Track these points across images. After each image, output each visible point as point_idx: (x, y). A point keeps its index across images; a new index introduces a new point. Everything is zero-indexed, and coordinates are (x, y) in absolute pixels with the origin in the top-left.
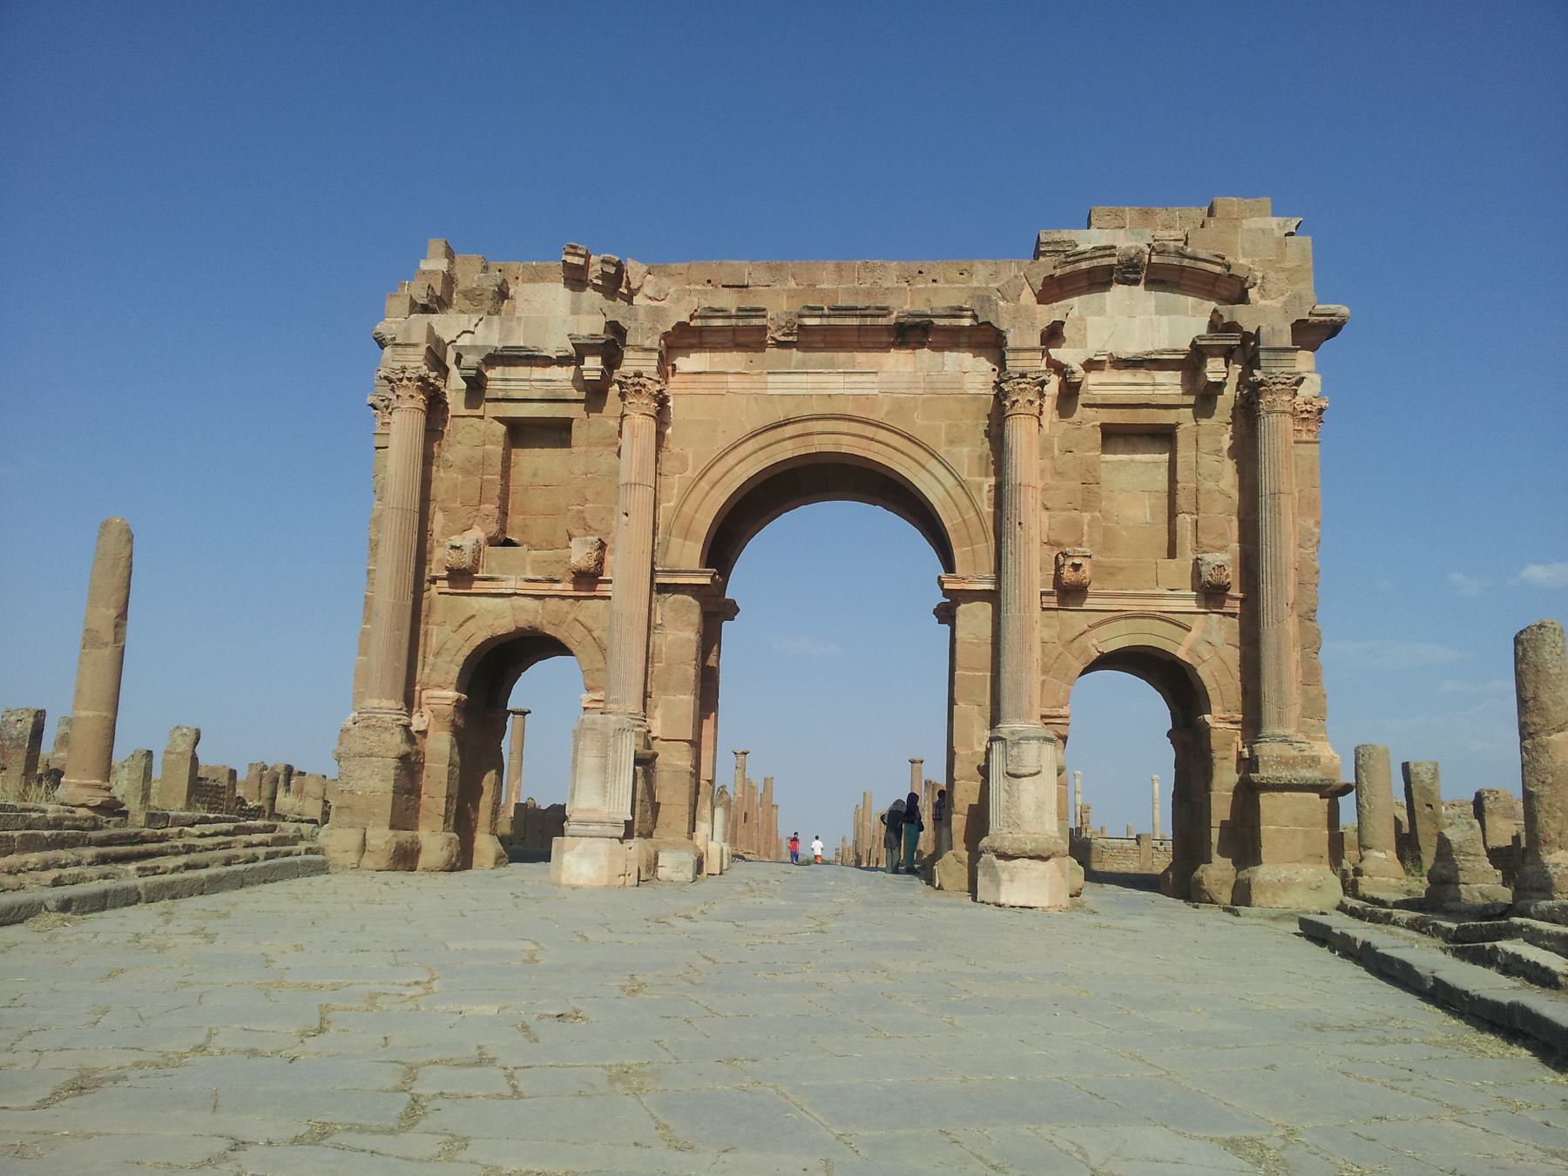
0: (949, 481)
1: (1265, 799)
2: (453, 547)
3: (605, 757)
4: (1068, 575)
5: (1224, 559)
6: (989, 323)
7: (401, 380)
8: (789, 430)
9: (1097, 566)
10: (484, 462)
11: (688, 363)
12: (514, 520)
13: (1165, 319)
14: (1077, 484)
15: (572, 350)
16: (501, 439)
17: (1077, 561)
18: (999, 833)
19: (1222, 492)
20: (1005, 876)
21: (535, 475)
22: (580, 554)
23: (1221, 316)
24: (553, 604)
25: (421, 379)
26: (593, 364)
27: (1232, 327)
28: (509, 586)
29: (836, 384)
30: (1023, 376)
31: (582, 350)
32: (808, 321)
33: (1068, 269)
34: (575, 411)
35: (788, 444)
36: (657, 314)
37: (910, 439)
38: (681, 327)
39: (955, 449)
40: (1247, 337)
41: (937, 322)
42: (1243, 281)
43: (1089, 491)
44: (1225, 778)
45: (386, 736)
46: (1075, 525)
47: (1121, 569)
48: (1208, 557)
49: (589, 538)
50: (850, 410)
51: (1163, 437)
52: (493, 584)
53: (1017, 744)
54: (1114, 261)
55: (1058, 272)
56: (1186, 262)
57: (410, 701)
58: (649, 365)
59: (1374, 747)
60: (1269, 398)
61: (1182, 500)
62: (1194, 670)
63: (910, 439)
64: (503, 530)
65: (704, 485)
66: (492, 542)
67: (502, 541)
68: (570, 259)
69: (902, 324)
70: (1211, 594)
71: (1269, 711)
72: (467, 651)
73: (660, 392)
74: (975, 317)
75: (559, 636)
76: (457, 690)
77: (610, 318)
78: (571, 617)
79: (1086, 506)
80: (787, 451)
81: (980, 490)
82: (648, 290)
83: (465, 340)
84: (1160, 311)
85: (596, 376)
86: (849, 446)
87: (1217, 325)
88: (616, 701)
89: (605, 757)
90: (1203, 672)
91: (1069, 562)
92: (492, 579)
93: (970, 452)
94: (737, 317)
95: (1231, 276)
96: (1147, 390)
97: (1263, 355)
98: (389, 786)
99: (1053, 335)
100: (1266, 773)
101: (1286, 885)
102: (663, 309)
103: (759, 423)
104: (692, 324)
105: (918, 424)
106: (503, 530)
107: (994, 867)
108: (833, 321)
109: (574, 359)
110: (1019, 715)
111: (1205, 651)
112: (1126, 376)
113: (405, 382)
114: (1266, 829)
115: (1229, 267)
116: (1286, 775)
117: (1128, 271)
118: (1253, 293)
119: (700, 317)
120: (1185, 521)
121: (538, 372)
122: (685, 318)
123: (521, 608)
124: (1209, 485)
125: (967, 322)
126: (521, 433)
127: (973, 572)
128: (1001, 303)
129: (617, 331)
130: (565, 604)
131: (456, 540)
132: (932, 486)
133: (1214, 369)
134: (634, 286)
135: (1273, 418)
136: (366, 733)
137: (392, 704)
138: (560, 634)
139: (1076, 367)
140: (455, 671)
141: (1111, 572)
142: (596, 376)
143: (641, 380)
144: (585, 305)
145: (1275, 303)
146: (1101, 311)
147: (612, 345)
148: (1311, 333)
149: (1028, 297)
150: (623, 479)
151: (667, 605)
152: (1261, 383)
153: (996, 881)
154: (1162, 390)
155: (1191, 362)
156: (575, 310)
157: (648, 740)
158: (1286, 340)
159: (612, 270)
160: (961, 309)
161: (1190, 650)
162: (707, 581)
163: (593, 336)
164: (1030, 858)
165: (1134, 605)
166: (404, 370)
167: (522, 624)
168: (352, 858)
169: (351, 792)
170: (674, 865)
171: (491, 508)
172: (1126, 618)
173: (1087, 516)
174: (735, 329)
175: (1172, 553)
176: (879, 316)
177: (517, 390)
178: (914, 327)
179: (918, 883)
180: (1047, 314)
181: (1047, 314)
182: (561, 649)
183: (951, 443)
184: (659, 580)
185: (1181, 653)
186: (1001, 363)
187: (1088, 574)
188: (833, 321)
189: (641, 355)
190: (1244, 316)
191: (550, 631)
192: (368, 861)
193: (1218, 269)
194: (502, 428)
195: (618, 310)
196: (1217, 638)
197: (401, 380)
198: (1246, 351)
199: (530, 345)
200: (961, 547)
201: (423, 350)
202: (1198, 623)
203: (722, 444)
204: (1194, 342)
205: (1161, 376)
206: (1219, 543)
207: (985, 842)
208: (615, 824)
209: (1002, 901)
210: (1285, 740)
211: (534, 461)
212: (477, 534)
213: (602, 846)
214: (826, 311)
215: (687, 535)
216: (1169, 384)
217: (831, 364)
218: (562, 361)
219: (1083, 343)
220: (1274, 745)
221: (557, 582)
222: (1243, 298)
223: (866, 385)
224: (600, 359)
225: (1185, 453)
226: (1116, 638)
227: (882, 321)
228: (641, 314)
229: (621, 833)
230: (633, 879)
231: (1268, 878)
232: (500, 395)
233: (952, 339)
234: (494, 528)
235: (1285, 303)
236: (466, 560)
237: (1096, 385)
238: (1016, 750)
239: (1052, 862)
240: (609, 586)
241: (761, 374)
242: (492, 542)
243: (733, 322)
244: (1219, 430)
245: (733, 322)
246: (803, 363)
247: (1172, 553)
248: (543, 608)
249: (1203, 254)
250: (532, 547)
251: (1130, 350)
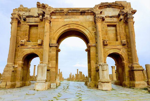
0: (89, 32)
1: (135, 72)
2: (21, 41)
3: (42, 70)
4: (105, 43)
5: (124, 41)
6: (93, 12)
7: (14, 18)
8: (67, 26)
9: (109, 42)
10: (26, 30)
11: (54, 17)
12: (30, 38)
13: (114, 12)
14: (105, 32)
15: (38, 15)
16: (29, 28)
17: (107, 41)
18: (101, 79)
19: (123, 33)
20: (103, 86)
21: (33, 33)
22: (39, 42)
23: (121, 11)
24: (35, 49)
25: (17, 18)
26: (41, 17)
27: (123, 12)
28: (30, 46)
29: (73, 19)
30: (98, 17)
31: (39, 15)
32: (69, 12)
33: (102, 5)
35: (67, 27)
36: (49, 11)
37: (83, 26)
38: (53, 12)
39: (89, 28)
40: (125, 13)
41: (86, 12)
42: (124, 6)
43: (106, 33)
44: (127, 69)
45: (10, 68)
46: (105, 37)
47: (111, 43)
48: (123, 41)
49: (40, 40)
50: (75, 23)
51: (115, 26)
52: (27, 47)
53: (103, 66)
54: (108, 4)
55: (101, 6)
56: (116, 4)
57: (14, 63)
58: (49, 16)
59: (148, 64)
60: (129, 20)
61: (118, 34)
62: (121, 55)
63: (83, 26)
64: (29, 40)
65: (56, 33)
66: (27, 41)
67: (29, 41)
68: (38, 4)
69: (82, 12)
72: (23, 56)
73: (50, 20)
74: (91, 11)
75: (36, 54)
76: (22, 61)
77: (43, 11)
78: (38, 51)
79: (106, 35)
80: (67, 28)
81: (93, 33)
82: (48, 8)
83: (24, 14)
85: (41, 18)
86: (75, 27)
87: (121, 11)
88: (44, 62)
89: (42, 70)
90: (123, 56)
91: (105, 41)
92: (27, 46)
94: (60, 11)
95: (122, 6)
96: (113, 20)
97: (128, 15)
98: (10, 76)
99: (101, 12)
100: (135, 69)
101: (139, 84)
102: (50, 10)
103: (63, 25)
104: (54, 12)
105: (84, 25)
106: (29, 40)
107: (101, 84)
108: (73, 12)
109: (38, 17)
110: (101, 62)
111: (123, 53)
112: (110, 19)
113: (14, 19)
114: (136, 76)
115: (122, 5)
116: (138, 69)
118: (125, 8)
119: (55, 11)
120: (119, 37)
121: (34, 19)
122: (53, 11)
123: (31, 50)
124: (121, 32)
125: (90, 12)
126: (31, 26)
127: (92, 43)
128: (94, 9)
129: (44, 13)
130: (37, 49)
131: (22, 41)
132: (87, 33)
133: (122, 17)
134: (46, 7)
135: (130, 22)
136: (7, 68)
137: (12, 63)
138: (36, 53)
139: (104, 17)
140: (22, 59)
141: (110, 43)
142: (41, 18)
143: (47, 18)
144: (40, 10)
145: (128, 9)
146: (106, 11)
147: (43, 14)
149: (97, 8)
150: (45, 31)
151: (51, 49)
152: (128, 18)
153: (101, 86)
154: (114, 20)
156: (38, 11)
157: (48, 67)
158: (131, 13)
159: (43, 5)
160: (89, 10)
161: (121, 53)
162: (57, 45)
163: (41, 13)
164: (107, 83)
165: (114, 47)
166: (14, 17)
167: (31, 52)
168: (4, 87)
169: (5, 77)
170: (53, 85)
171: (27, 36)
172: (113, 49)
173: (106, 36)
174: (60, 13)
175: (117, 40)
176: (78, 11)
178: (83, 12)
179: (95, 89)
180: (100, 10)
181: (100, 10)
182: (38, 56)
183: (88, 27)
184: (50, 45)
185: (120, 53)
186: (95, 16)
187: (108, 43)
188: (73, 12)
189: (47, 15)
190: (125, 11)
191: (35, 53)
192: (7, 87)
193: (120, 5)
194: (28, 26)
195: (44, 10)
196: (124, 51)
197: (14, 18)
198: (126, 15)
199: (32, 15)
200: (90, 40)
201: (17, 14)
202: (122, 49)
203: (58, 27)
204: (119, 13)
205: (114, 19)
206: (123, 39)
207: (99, 80)
208: (44, 80)
209: (103, 89)
210: (137, 64)
211: (33, 30)
212: (25, 40)
213: (41, 84)
214: (72, 10)
215: (54, 39)
218: (36, 17)
219: (104, 14)
220: (135, 65)
221: (36, 46)
222: (124, 9)
224: (42, 16)
225: (118, 28)
226: (112, 52)
227: (79, 12)
228: (47, 11)
229: (45, 82)
230: (47, 89)
231: (137, 83)
232: (28, 22)
234: (27, 39)
235: (129, 9)
236: (23, 43)
237: (106, 20)
238: (103, 67)
239: (109, 83)
240: (43, 46)
241: (63, 19)
242: (27, 41)
243: (60, 12)
245: (60, 12)
246: (69, 17)
248: (34, 50)
249: (118, 4)
250: (33, 42)
251: (110, 15)
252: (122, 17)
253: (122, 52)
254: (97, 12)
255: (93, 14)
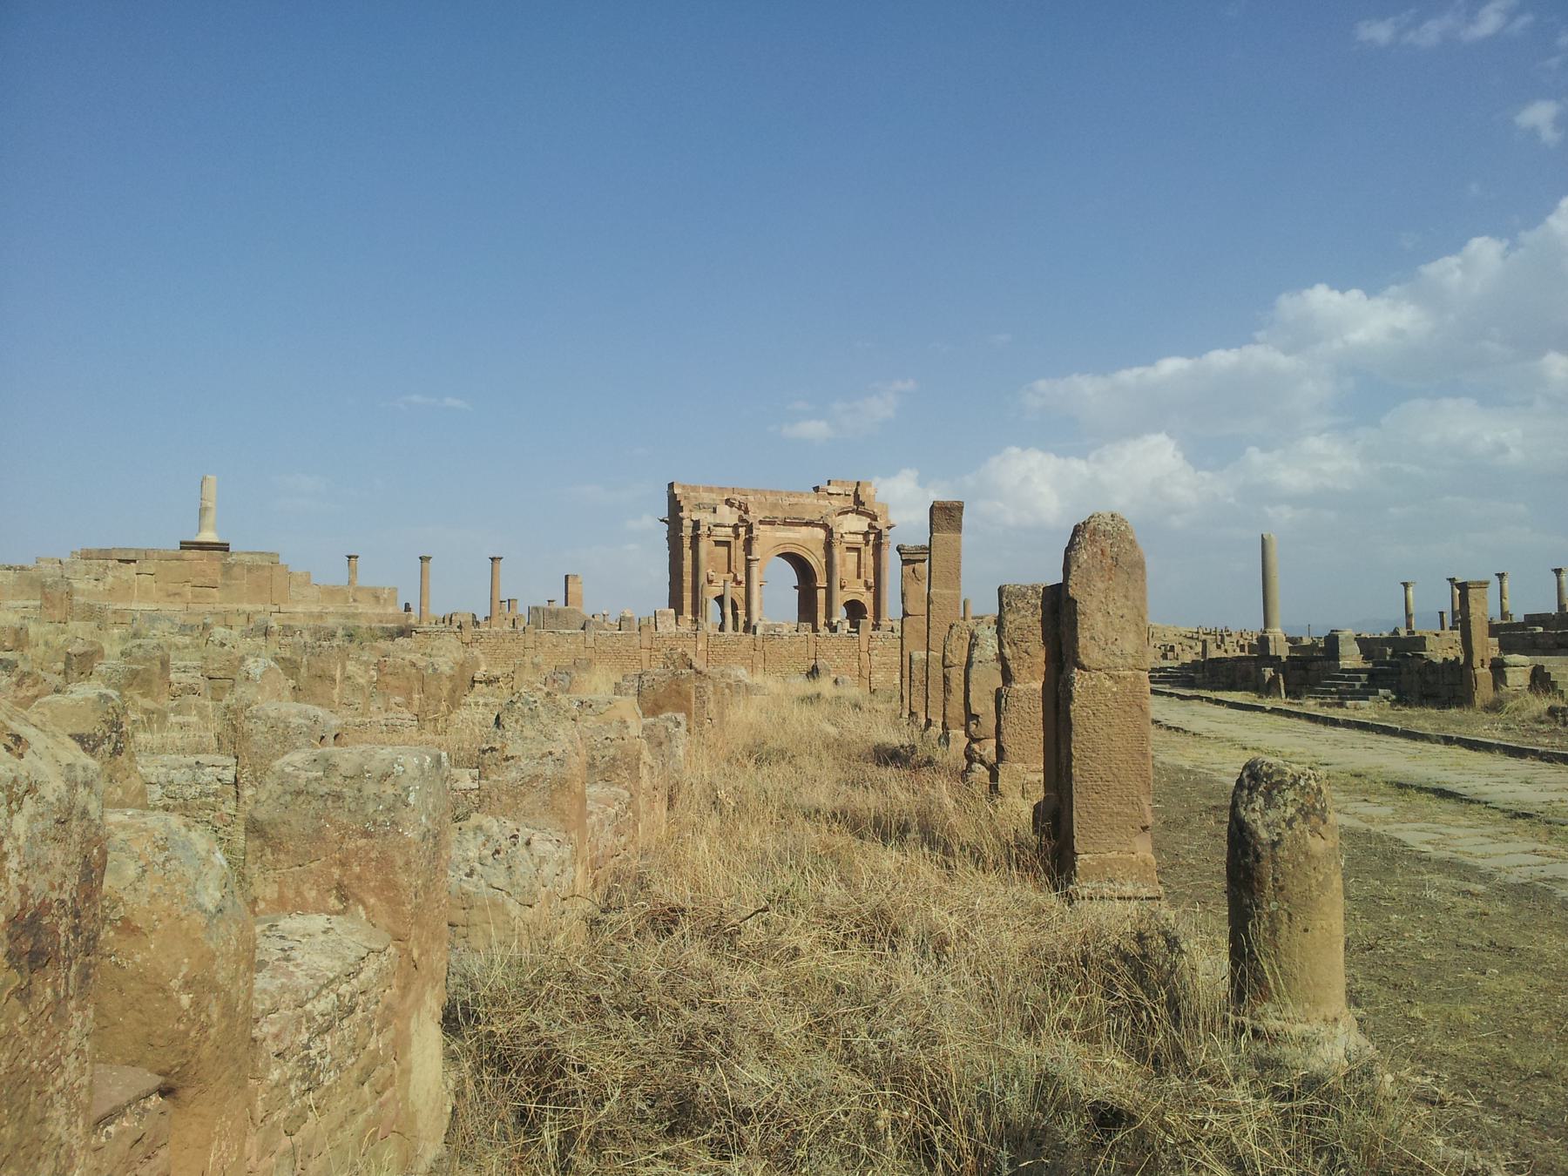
27: (875, 528)
34: (732, 540)
43: (844, 560)
51: (858, 550)
61: (862, 566)
70: (868, 588)
71: (882, 614)
84: (859, 520)
87: (870, 526)
93: (820, 553)
112: (852, 536)
117: (852, 512)
120: (862, 570)
126: (718, 543)
148: (889, 528)
155: (866, 534)
175: (859, 577)
177: (718, 534)
216: (860, 538)
217: (790, 530)
222: (876, 520)
223: (798, 536)
233: (817, 525)
244: (870, 550)
247: (859, 577)
252: (872, 537)
253: (867, 599)
254: (834, 521)
255: (825, 527)
